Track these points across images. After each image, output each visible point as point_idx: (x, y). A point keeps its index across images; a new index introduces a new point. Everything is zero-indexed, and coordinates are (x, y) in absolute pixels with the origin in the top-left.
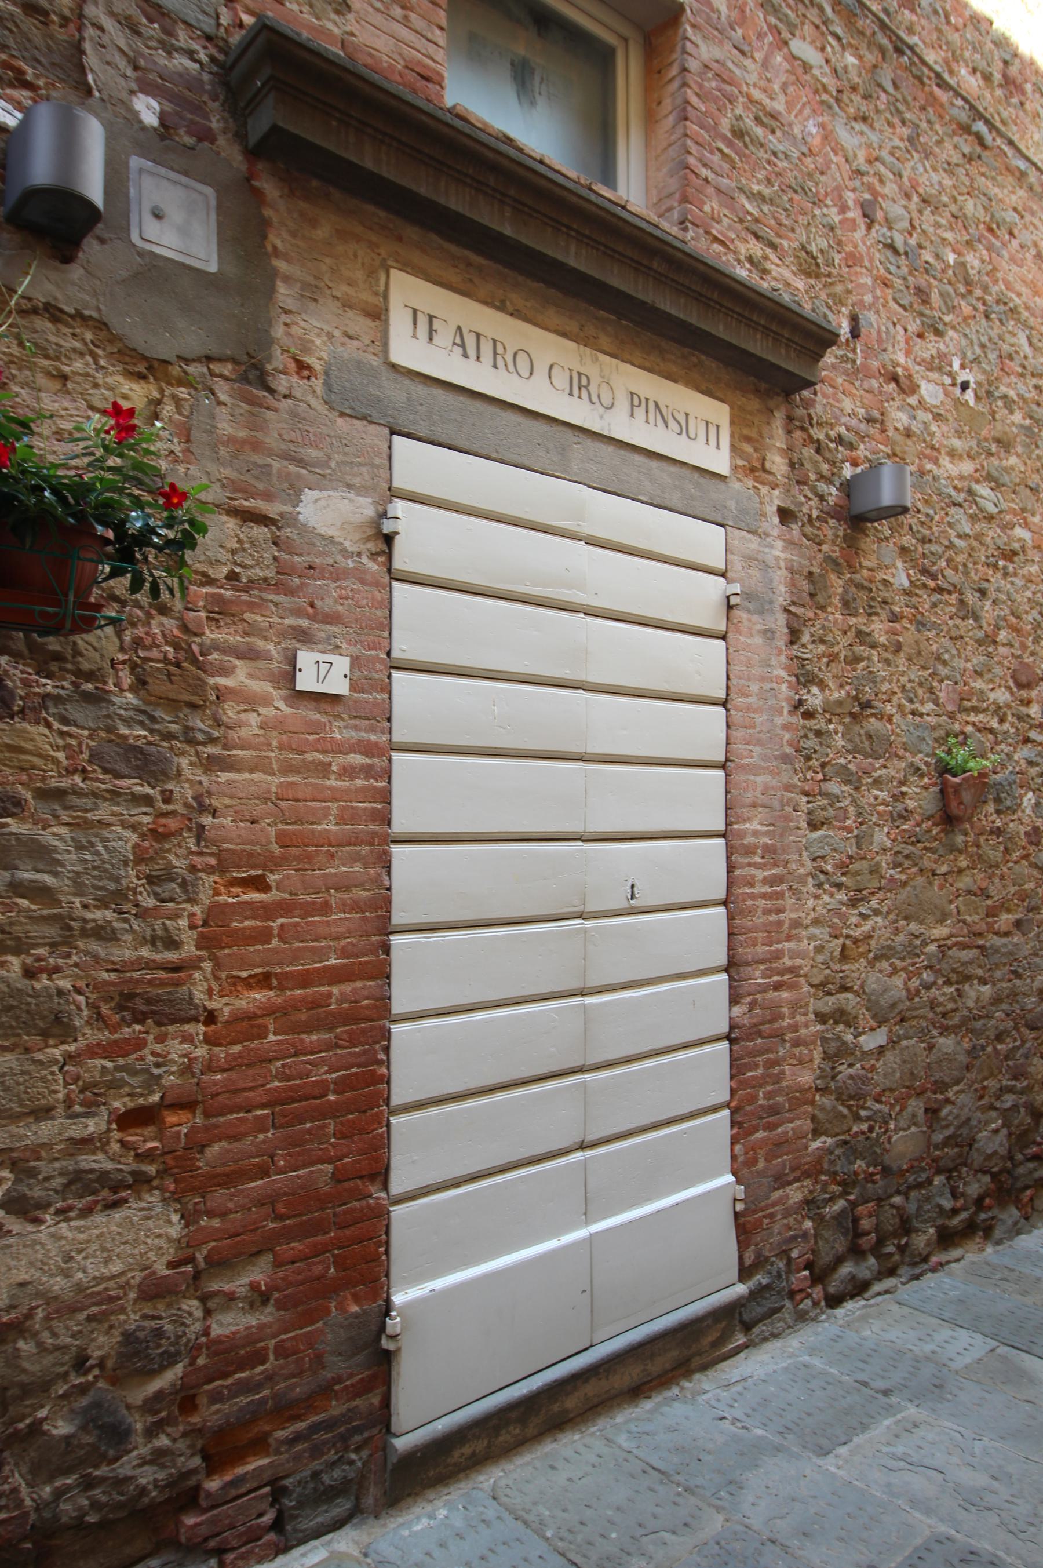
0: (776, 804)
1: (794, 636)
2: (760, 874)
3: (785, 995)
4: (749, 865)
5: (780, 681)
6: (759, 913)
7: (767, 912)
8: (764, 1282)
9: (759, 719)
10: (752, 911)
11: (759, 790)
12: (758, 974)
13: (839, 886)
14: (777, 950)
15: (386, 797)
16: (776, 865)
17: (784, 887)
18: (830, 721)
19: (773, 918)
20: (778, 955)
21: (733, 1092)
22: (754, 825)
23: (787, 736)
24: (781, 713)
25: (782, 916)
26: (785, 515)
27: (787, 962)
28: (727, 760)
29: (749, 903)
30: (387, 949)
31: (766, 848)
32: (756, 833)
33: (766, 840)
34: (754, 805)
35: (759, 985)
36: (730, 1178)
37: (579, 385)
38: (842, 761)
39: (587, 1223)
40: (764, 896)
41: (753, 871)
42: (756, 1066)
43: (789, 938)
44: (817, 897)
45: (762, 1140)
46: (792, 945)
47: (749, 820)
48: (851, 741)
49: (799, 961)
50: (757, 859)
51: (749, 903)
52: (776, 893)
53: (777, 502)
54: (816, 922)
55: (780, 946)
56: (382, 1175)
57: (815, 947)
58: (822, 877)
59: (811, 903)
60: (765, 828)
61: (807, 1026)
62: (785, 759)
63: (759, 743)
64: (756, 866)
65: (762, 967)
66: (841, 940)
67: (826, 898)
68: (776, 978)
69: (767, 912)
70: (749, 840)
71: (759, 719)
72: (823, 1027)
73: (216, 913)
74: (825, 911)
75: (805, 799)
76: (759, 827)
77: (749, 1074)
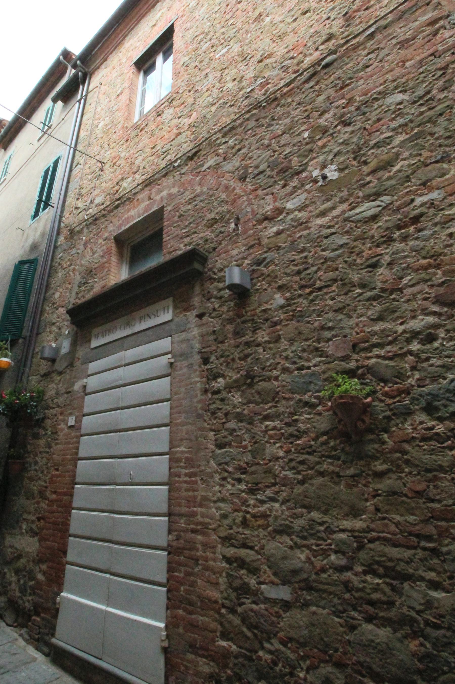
0: (193, 438)
1: (206, 361)
2: (184, 471)
3: (199, 537)
4: (178, 467)
6: (183, 490)
7: (187, 490)
9: (184, 402)
10: (179, 489)
11: (184, 432)
12: (182, 521)
13: (239, 481)
14: (193, 512)
15: (78, 448)
16: (193, 467)
17: (198, 478)
18: (231, 392)
19: (191, 494)
20: (194, 514)
21: (168, 580)
22: (182, 449)
23: (200, 406)
24: (196, 396)
25: (196, 493)
26: (200, 316)
28: (171, 422)
29: (177, 485)
30: (73, 488)
31: (187, 459)
32: (182, 452)
33: (187, 455)
34: (182, 440)
35: (182, 527)
37: (128, 324)
38: (239, 410)
39: (108, 606)
40: (186, 482)
41: (180, 470)
42: (180, 571)
43: (201, 506)
44: (222, 486)
46: (203, 510)
47: (179, 446)
48: (246, 398)
49: (207, 520)
50: (182, 464)
51: (177, 485)
52: (193, 481)
53: (194, 314)
54: (222, 500)
55: (195, 509)
57: (220, 515)
58: (226, 474)
59: (217, 488)
60: (186, 450)
61: (214, 560)
62: (199, 416)
63: (185, 412)
64: (182, 467)
65: (184, 518)
66: (241, 514)
67: (229, 487)
68: (192, 526)
69: (187, 490)
70: (178, 455)
71: (184, 402)
72: (228, 566)
74: (227, 494)
75: (212, 433)
76: (184, 449)
77: (176, 574)
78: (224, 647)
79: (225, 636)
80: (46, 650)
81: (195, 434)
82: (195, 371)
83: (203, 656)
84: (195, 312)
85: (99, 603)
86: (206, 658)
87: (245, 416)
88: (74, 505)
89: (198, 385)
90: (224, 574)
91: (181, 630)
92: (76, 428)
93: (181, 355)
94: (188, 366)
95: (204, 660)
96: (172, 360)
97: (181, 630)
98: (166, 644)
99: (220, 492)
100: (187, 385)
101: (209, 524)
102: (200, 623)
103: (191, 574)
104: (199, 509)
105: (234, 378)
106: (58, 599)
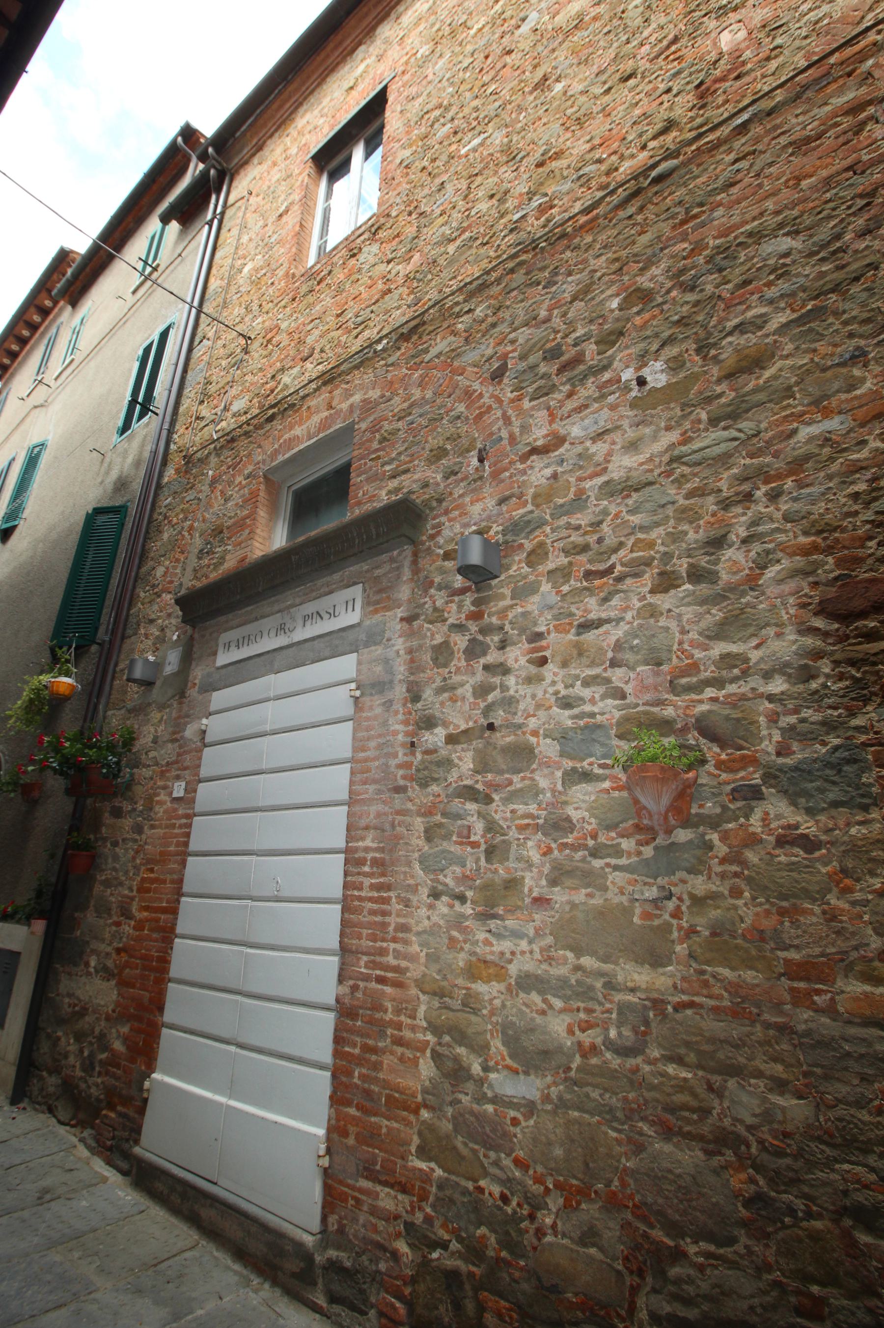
2: (367, 882)
3: (388, 990)
4: (359, 874)
5: (395, 733)
6: (365, 912)
7: (373, 912)
8: (348, 1264)
10: (358, 911)
12: (362, 963)
13: (462, 899)
14: (381, 948)
15: (188, 835)
17: (391, 894)
19: (378, 919)
20: (383, 952)
22: (368, 843)
23: (401, 772)
24: (396, 756)
27: (391, 960)
31: (375, 862)
32: (367, 849)
34: (367, 828)
36: (321, 1132)
39: (230, 1098)
40: (371, 899)
41: (361, 879)
42: (354, 1045)
43: (394, 940)
44: (431, 907)
45: (354, 1117)
46: (398, 946)
47: (363, 839)
49: (404, 964)
50: (366, 869)
51: (356, 903)
52: (382, 898)
55: (385, 945)
56: (161, 1009)
59: (423, 912)
60: (375, 845)
61: (413, 1028)
63: (375, 781)
64: (366, 875)
68: (378, 972)
69: (373, 912)
70: (360, 854)
73: (143, 880)
78: (421, 1170)
79: (423, 1152)
80: (125, 1166)
81: (390, 818)
82: (396, 713)
83: (385, 1184)
84: (400, 613)
85: (215, 1091)
86: (392, 1186)
87: (478, 791)
88: (179, 930)
89: (400, 737)
90: (428, 1053)
91: (351, 1141)
92: (189, 800)
93: (373, 685)
94: (384, 704)
95: (387, 1190)
96: (358, 693)
97: (351, 1141)
98: (325, 1162)
99: (429, 918)
100: (380, 736)
101: (407, 969)
102: (384, 1130)
103: (374, 1050)
104: (392, 946)
105: (463, 727)
106: (147, 1084)
